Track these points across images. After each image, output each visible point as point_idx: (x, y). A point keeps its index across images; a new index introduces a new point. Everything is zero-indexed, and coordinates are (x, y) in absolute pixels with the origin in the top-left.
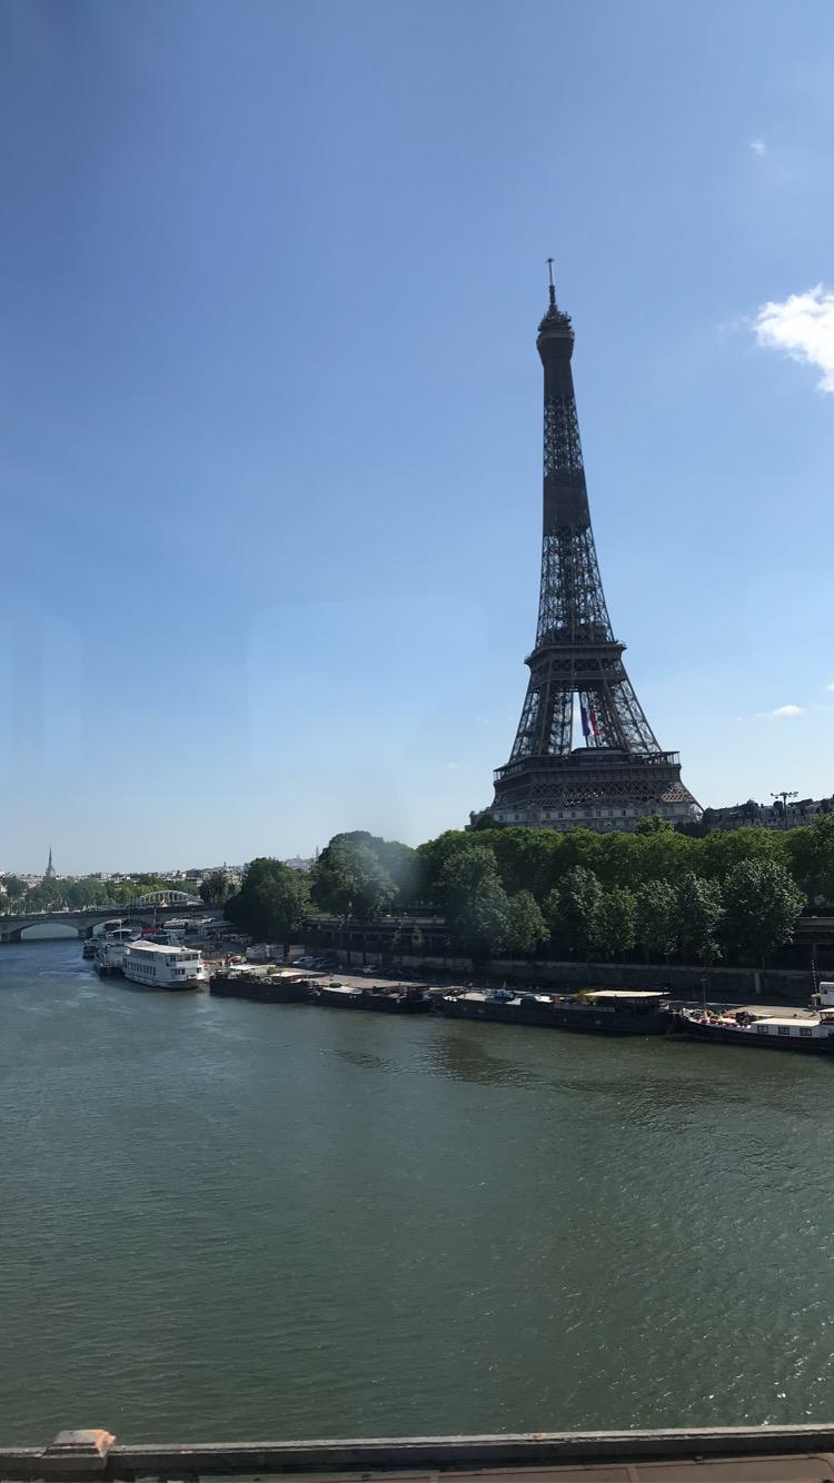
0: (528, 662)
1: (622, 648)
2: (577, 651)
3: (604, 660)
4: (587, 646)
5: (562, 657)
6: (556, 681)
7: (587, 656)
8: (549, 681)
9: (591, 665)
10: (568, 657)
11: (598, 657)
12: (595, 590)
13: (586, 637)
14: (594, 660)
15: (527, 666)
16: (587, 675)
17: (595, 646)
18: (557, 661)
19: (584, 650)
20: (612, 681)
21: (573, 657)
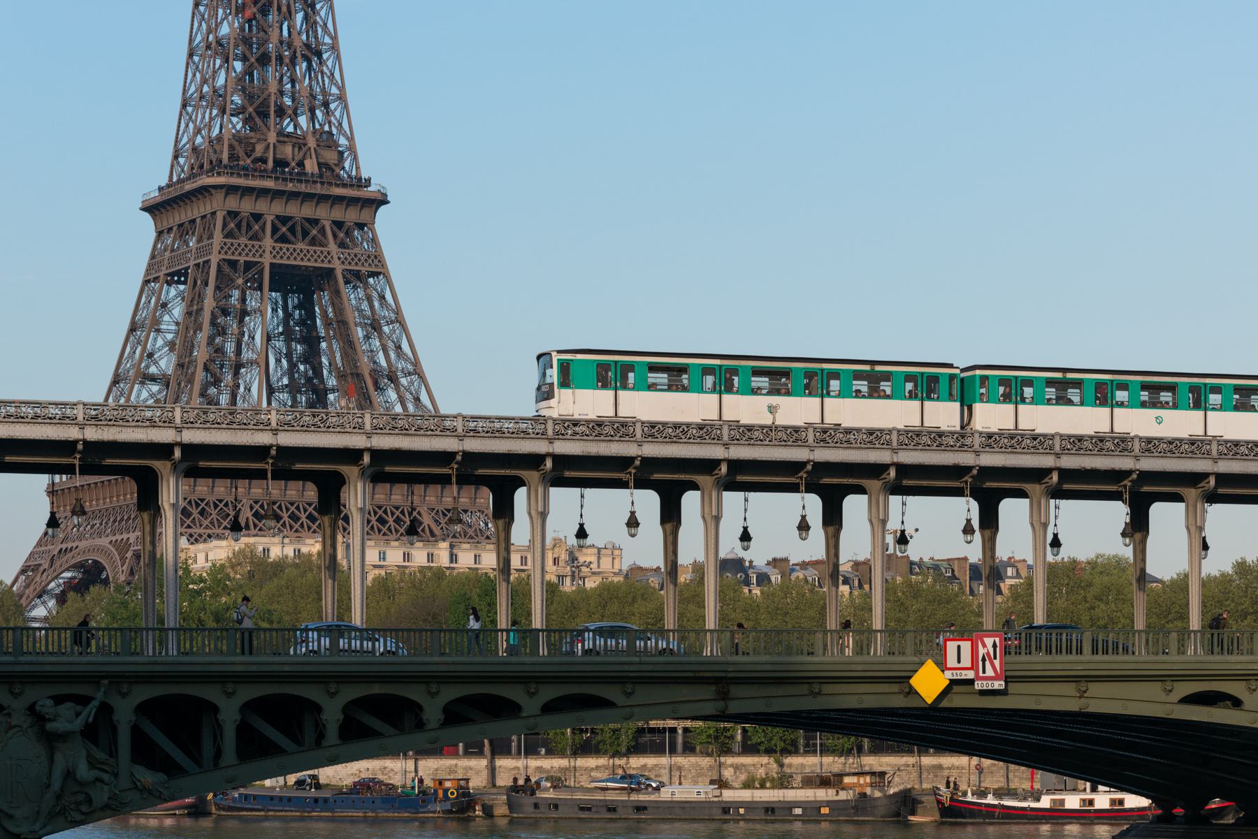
0: (151, 209)
1: (381, 201)
2: (276, 194)
3: (338, 224)
4: (302, 188)
5: (247, 206)
6: (233, 264)
7: (308, 211)
8: (214, 259)
9: (307, 230)
10: (262, 206)
11: (325, 214)
12: (319, 54)
13: (301, 164)
14: (314, 222)
15: (147, 215)
16: (300, 255)
17: (318, 189)
18: (232, 214)
19: (293, 195)
20: (358, 275)
21: (271, 210)
